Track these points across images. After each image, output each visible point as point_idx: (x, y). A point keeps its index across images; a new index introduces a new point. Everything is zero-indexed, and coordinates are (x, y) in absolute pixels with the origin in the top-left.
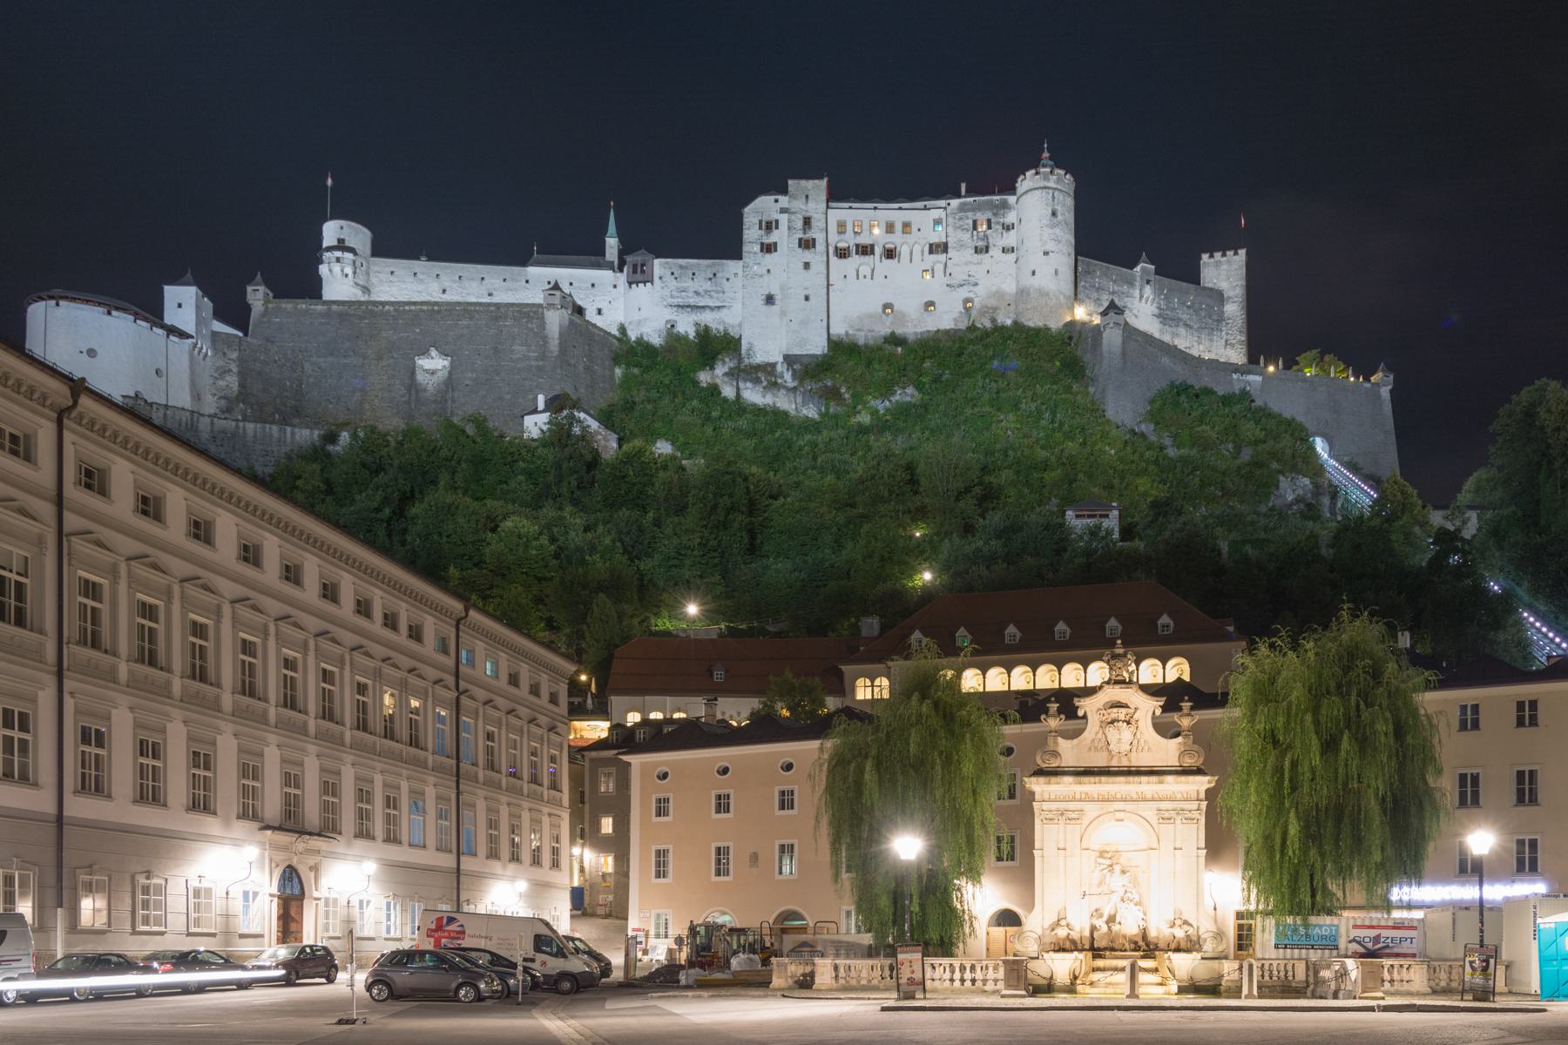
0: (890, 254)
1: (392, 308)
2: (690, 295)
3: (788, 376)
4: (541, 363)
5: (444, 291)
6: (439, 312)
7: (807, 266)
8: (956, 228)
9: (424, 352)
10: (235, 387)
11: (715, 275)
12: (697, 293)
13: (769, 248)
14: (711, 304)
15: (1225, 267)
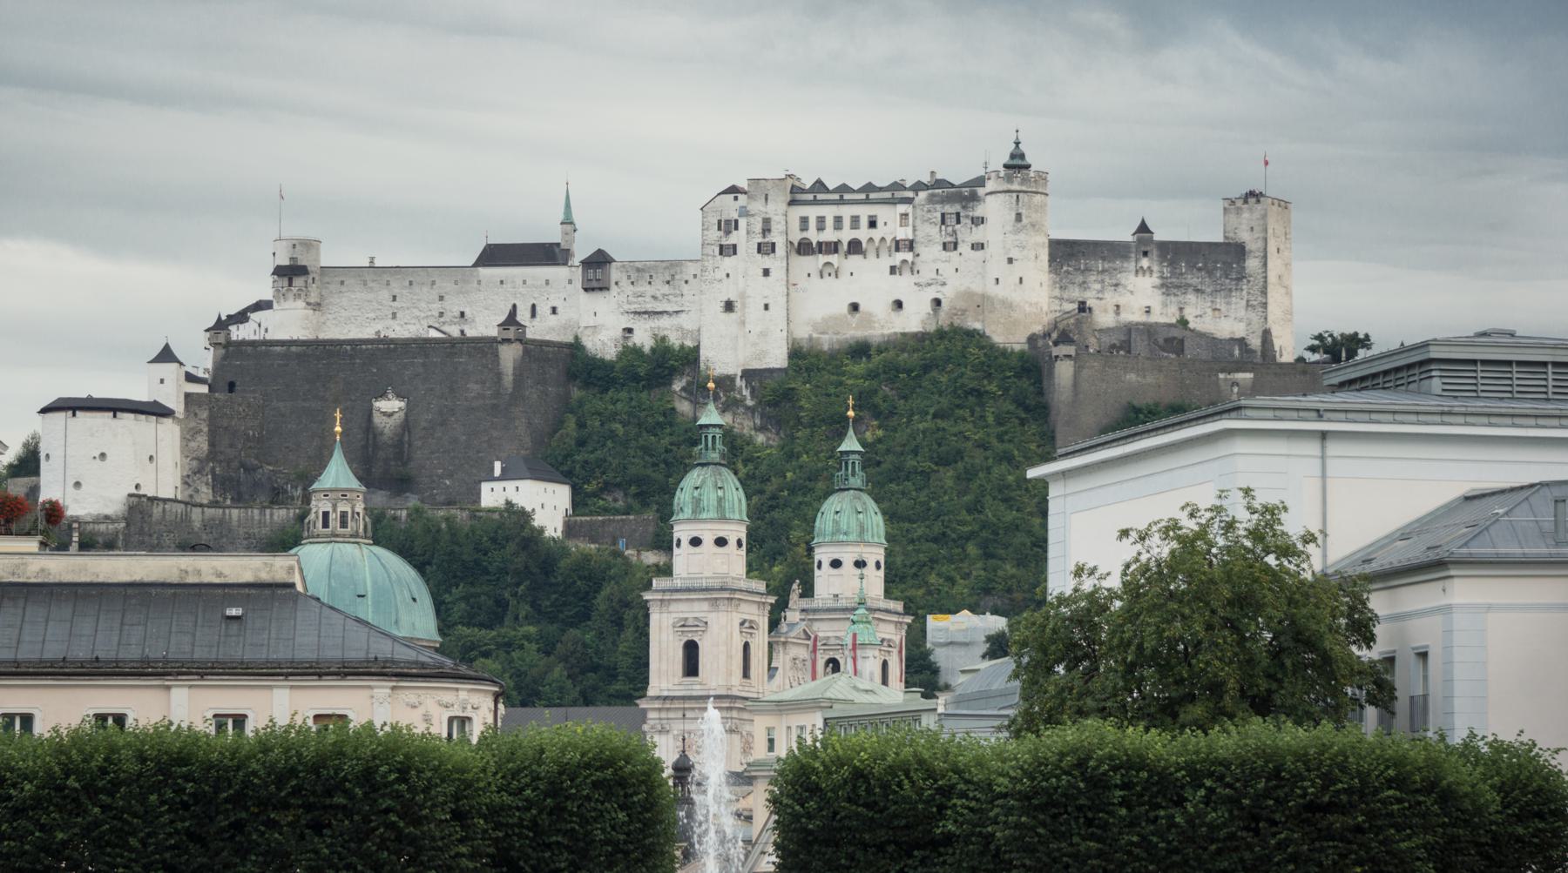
0: (855, 247)
1: (349, 347)
2: (648, 299)
3: (746, 393)
4: (495, 402)
5: (394, 298)
6: (395, 350)
7: (766, 272)
8: (924, 221)
9: (382, 395)
10: (205, 447)
11: (673, 275)
12: (654, 297)
13: (728, 250)
14: (669, 309)
15: (1246, 215)
